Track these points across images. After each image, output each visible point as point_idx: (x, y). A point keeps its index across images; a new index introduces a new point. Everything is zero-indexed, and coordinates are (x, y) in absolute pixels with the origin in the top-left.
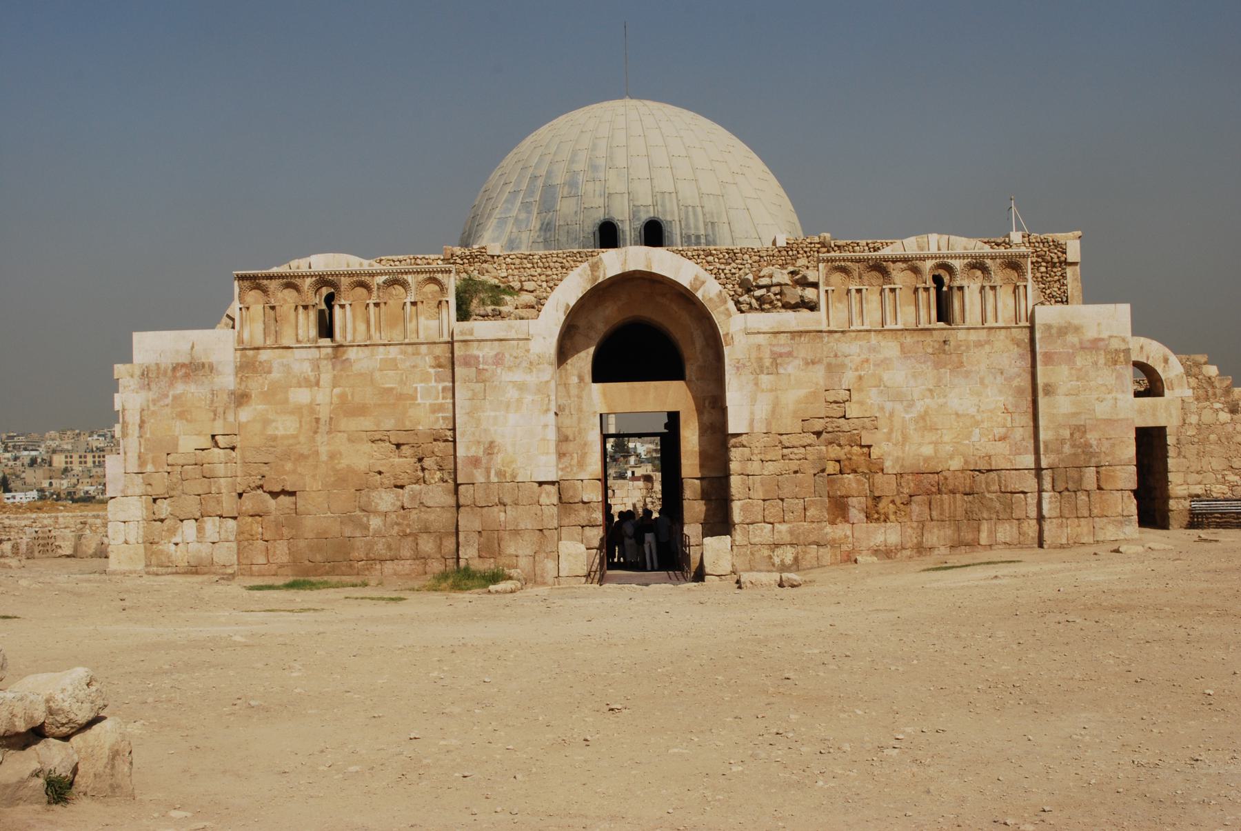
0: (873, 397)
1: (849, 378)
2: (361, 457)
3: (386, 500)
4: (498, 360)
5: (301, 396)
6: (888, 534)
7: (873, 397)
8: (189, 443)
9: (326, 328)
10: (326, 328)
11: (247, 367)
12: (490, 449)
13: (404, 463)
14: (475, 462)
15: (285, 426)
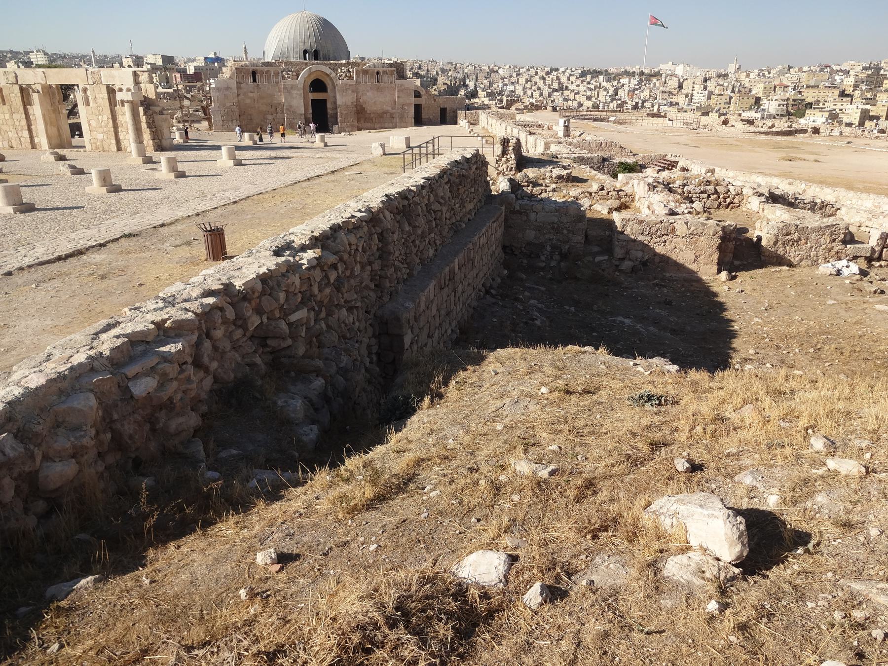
0: (364, 98)
1: (360, 93)
2: (264, 108)
3: (270, 117)
4: (292, 88)
5: (251, 95)
6: (369, 125)
7: (364, 98)
8: (228, 104)
9: (254, 80)
10: (254, 80)
11: (238, 88)
12: (291, 106)
13: (273, 109)
14: (287, 109)
15: (248, 101)
